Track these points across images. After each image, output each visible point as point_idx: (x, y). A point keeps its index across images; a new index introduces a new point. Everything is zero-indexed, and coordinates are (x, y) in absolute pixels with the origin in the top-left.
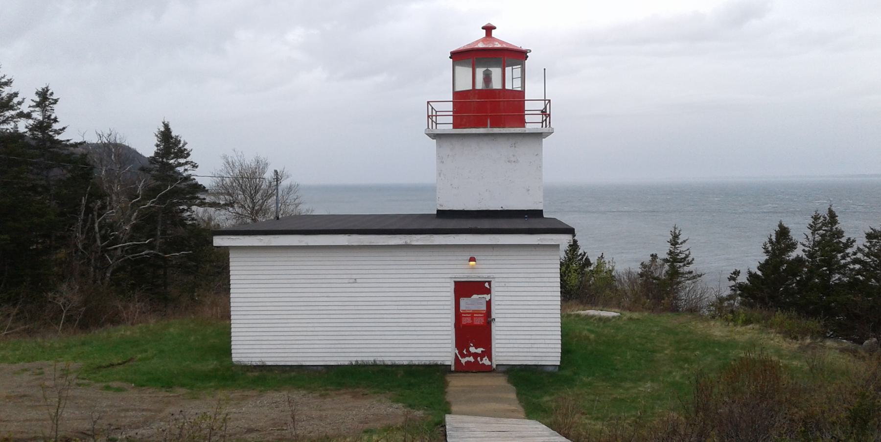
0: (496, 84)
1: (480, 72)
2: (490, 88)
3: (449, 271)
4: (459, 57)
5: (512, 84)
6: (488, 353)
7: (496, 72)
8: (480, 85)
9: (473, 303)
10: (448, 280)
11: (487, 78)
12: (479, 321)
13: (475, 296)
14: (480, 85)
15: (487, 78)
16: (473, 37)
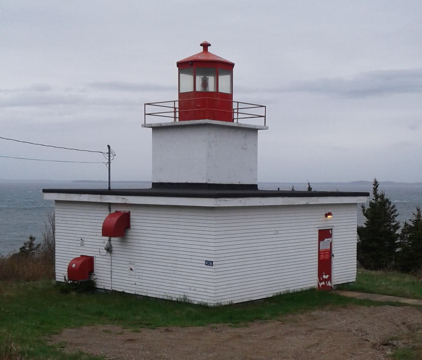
0: (211, 88)
1: (199, 79)
2: (207, 90)
3: (317, 223)
4: (184, 66)
5: (224, 88)
6: (330, 279)
7: (211, 80)
8: (199, 88)
9: (325, 245)
10: (314, 229)
11: (205, 84)
12: (327, 257)
13: (326, 240)
14: (199, 88)
15: (205, 84)
16: (194, 51)
